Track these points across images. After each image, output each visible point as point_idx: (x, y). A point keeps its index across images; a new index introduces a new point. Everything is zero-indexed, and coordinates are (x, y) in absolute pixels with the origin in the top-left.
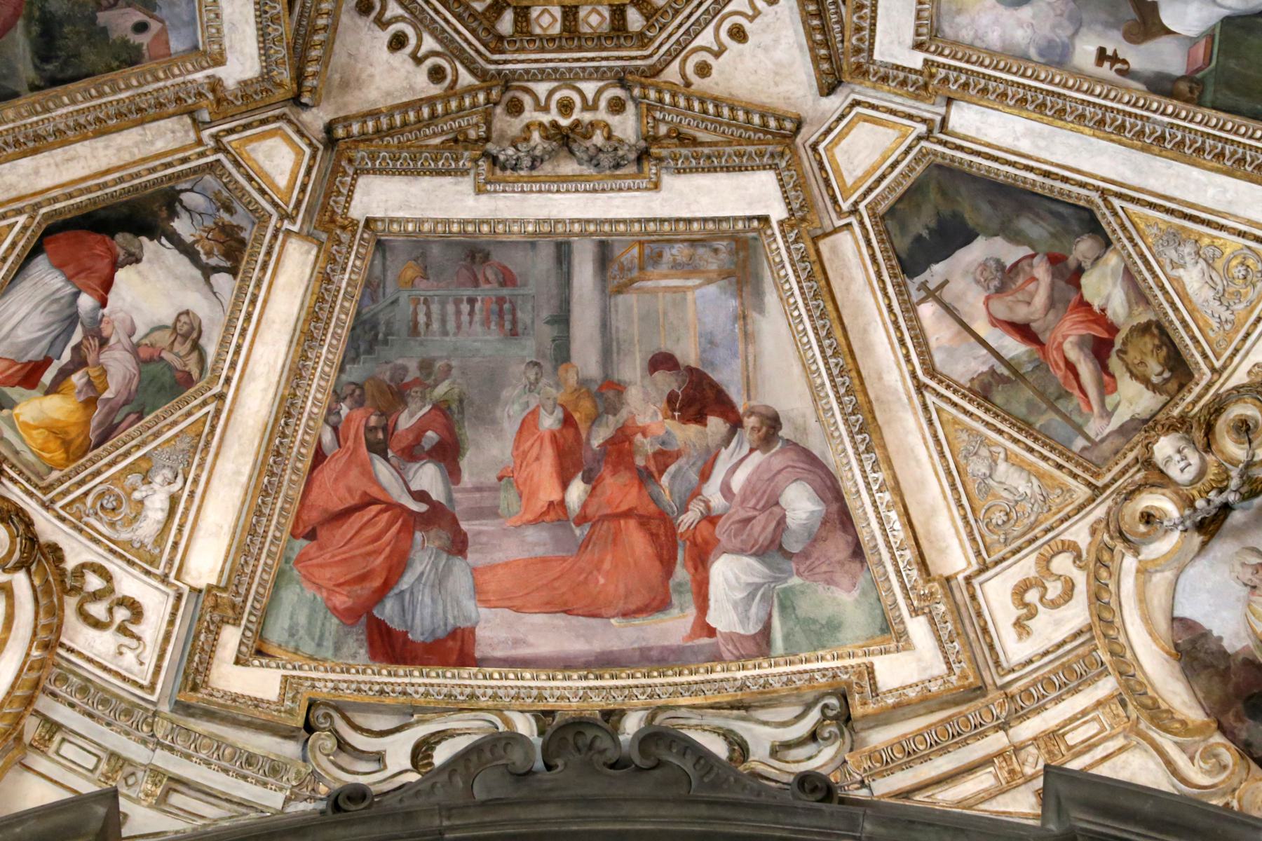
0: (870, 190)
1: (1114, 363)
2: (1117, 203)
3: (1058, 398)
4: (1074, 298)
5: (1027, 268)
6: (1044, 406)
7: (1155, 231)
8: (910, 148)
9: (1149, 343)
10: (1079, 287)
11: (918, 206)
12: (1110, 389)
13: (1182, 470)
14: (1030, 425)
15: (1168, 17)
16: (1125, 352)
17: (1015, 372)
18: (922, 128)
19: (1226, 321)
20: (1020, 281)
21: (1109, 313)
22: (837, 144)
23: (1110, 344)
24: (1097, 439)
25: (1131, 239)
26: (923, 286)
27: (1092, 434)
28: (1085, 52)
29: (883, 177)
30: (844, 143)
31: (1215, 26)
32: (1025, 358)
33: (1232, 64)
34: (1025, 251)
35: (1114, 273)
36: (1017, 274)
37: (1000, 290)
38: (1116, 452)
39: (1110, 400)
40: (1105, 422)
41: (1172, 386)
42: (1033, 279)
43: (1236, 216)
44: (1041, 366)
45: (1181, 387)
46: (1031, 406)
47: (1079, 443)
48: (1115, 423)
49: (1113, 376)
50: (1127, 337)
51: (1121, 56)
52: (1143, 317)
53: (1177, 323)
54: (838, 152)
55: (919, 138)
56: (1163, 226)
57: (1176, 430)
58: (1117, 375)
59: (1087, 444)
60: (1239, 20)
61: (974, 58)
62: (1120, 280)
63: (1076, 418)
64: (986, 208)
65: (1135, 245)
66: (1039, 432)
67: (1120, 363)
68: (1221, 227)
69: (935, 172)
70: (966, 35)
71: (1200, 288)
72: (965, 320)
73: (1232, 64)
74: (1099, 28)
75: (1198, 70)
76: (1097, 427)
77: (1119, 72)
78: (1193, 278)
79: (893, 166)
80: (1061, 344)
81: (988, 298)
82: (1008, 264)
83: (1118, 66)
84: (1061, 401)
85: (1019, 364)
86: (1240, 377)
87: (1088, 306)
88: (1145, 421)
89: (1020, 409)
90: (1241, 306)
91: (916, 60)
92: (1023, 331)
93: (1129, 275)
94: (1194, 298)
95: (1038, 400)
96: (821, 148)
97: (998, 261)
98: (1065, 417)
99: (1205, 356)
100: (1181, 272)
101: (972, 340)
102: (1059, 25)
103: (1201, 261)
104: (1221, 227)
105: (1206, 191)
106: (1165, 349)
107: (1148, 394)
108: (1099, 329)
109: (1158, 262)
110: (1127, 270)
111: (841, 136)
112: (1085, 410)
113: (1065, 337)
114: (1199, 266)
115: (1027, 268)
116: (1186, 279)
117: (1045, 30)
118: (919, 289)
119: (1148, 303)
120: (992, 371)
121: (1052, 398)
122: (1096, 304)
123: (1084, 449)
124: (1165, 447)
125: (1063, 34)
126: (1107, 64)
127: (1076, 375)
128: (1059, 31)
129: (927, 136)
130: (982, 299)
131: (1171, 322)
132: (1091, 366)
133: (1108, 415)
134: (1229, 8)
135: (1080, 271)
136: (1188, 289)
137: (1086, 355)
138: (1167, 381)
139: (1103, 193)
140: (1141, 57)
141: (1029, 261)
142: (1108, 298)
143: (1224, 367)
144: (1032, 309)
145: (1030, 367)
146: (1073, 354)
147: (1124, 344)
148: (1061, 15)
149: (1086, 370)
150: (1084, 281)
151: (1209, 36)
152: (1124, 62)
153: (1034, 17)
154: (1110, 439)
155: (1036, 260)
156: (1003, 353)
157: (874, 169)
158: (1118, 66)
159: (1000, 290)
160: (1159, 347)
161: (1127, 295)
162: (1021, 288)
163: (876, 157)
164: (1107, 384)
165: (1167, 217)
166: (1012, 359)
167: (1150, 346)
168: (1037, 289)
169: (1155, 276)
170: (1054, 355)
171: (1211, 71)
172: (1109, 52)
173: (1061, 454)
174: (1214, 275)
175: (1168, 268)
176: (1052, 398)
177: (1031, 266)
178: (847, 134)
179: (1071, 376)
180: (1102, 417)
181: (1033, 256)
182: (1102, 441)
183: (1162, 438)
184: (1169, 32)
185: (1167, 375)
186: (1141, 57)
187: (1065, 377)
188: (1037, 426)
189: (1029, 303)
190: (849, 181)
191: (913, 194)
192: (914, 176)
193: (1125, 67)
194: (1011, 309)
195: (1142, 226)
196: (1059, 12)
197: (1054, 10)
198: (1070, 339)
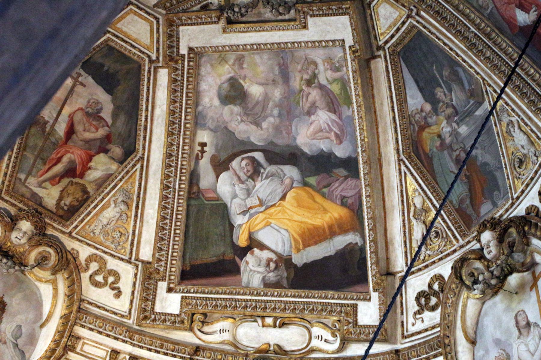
0: (117, 37)
1: (65, 181)
2: (138, 166)
3: (42, 159)
4: (93, 152)
5: (101, 125)
6: (36, 153)
7: (130, 187)
8: (143, 53)
9: (79, 195)
10: (98, 153)
11: (118, 61)
12: (53, 182)
13: (16, 237)
14: (25, 150)
15: (224, 176)
16: (72, 185)
17: (49, 134)
18: (154, 57)
19: (94, 233)
20: (94, 123)
21: (89, 172)
22: (135, 14)
23: (74, 176)
24: (26, 184)
25: (123, 177)
26: (80, 75)
27: (28, 181)
28: (203, 136)
29: (126, 42)
30: (136, 18)
31: (223, 200)
32: (57, 136)
33: (208, 211)
34: (109, 121)
35: (108, 169)
36: (98, 120)
37: (88, 114)
38: (22, 196)
39: (47, 184)
40: (36, 185)
41: (61, 212)
42: (97, 129)
43: (142, 226)
44: (56, 145)
45: (61, 217)
46: (35, 146)
47: (22, 176)
48: (37, 190)
49: (59, 182)
50: (80, 183)
51: (205, 155)
52: (89, 189)
53: (89, 209)
54: (131, 16)
55: (149, 57)
56: (132, 192)
57: (36, 228)
58: (60, 184)
59: (23, 180)
60: (226, 212)
61: (191, 79)
62: (105, 173)
63: (35, 170)
64: (125, 96)
65: (121, 180)
66: (22, 155)
67: (66, 184)
68: (135, 221)
69: (136, 66)
70: (203, 71)
71: (106, 218)
72: (68, 101)
73: (208, 211)
74: (215, 142)
75: (203, 195)
76: (32, 182)
77: (198, 154)
78: (111, 213)
79: (132, 46)
80: (68, 152)
81: (81, 109)
82: (102, 115)
83: (200, 154)
84: (41, 161)
85: (54, 134)
86: (70, 244)
87: (90, 160)
88: (41, 205)
89: (31, 143)
90: (102, 238)
91: (184, 51)
92: (71, 131)
93: (108, 178)
94: (101, 215)
95: (38, 149)
96: (131, 7)
97: (101, 109)
98: (34, 164)
99: (76, 227)
100: (113, 205)
101: (59, 108)
102: (213, 121)
103: (119, 214)
104: (135, 221)
105: (151, 209)
106: (78, 203)
107: (54, 202)
108: (80, 169)
109: (116, 192)
110: (112, 175)
111: (140, 16)
112: (40, 173)
113: (72, 153)
114: (117, 214)
115: (101, 125)
116: (109, 210)
117: (210, 114)
118: (77, 73)
119: (98, 189)
120: (46, 123)
121: (41, 156)
122: (92, 164)
123: (20, 179)
124: (26, 226)
125: (210, 124)
126: (199, 148)
127: (55, 164)
128: (210, 121)
129: (151, 61)
130: (81, 106)
131: (89, 206)
132: (62, 170)
133: (40, 185)
134: (231, 207)
135: (106, 151)
136: (105, 211)
137: (66, 166)
138: (62, 209)
139: (142, 158)
140: (205, 164)
141: (104, 123)
142: (96, 169)
143: (74, 238)
144: (82, 133)
145: (53, 140)
146: (65, 159)
147: (76, 183)
148: (218, 121)
149: (59, 168)
150: (102, 155)
151: (218, 198)
152: (202, 157)
153: (215, 107)
154: (29, 190)
155: (106, 128)
156: (57, 125)
157: (128, 37)
158: (200, 154)
159: (88, 114)
160: (78, 201)
161: (99, 178)
162: (91, 125)
163: (134, 36)
164: (54, 180)
165: (136, 193)
166: (55, 130)
167: (77, 196)
168: (93, 132)
169: (108, 193)
170: (63, 150)
171: (203, 201)
172: (205, 149)
173: (13, 172)
174: (114, 222)
175: (113, 199)
176: (41, 156)
177: (103, 126)
178: (142, 18)
179: (54, 162)
180: (38, 182)
181: (108, 126)
182: (27, 187)
183: (29, 223)
184: (217, 177)
185: (66, 208)
186: (205, 164)
187: (53, 159)
188: (25, 153)
189: (85, 130)
190: (119, 25)
191: (124, 58)
192: (131, 55)
193: (200, 158)
194: (79, 122)
195: (131, 180)
196: (219, 120)
197: (219, 117)
198: (72, 156)
